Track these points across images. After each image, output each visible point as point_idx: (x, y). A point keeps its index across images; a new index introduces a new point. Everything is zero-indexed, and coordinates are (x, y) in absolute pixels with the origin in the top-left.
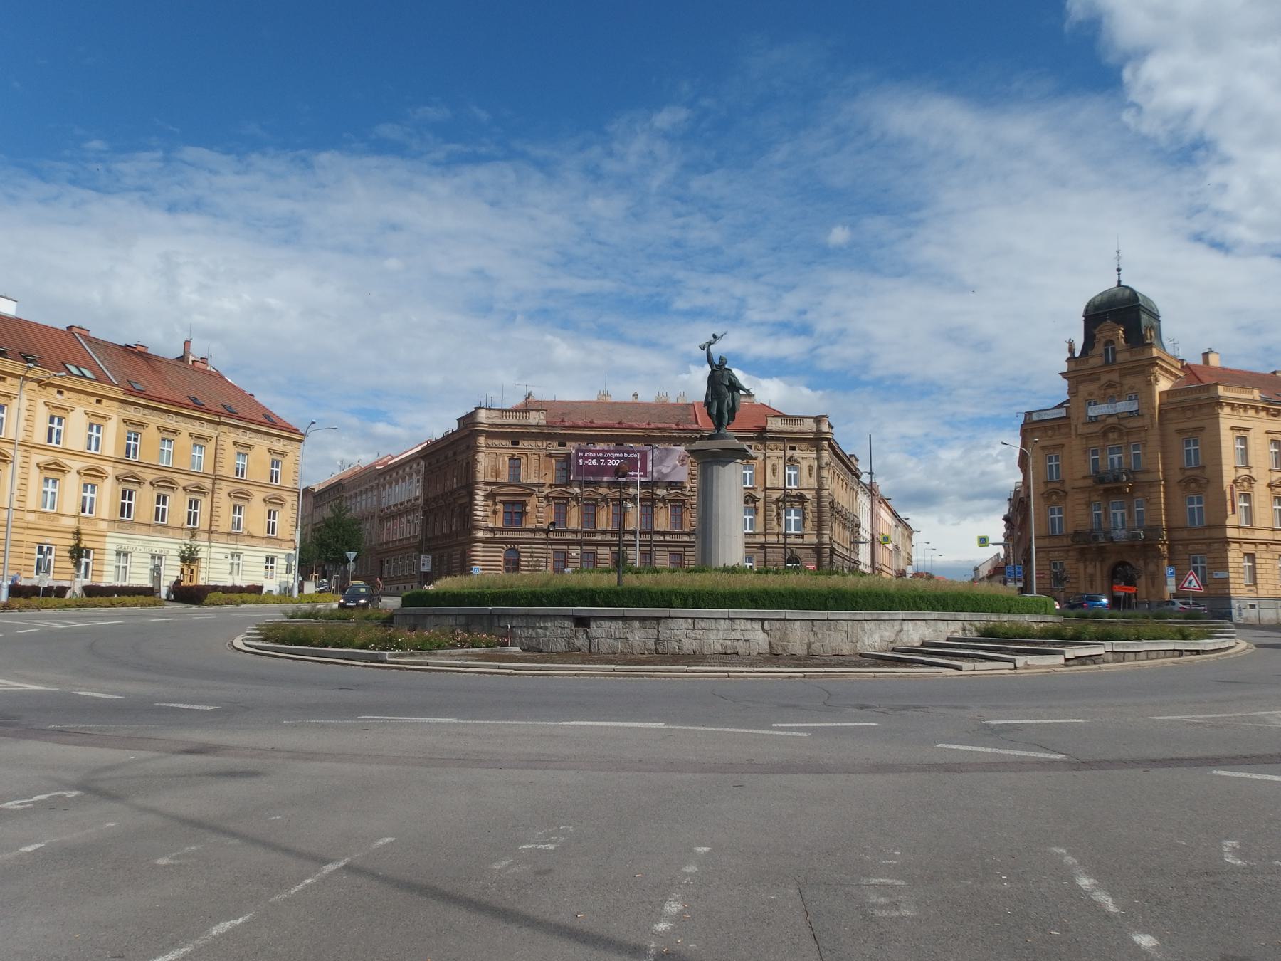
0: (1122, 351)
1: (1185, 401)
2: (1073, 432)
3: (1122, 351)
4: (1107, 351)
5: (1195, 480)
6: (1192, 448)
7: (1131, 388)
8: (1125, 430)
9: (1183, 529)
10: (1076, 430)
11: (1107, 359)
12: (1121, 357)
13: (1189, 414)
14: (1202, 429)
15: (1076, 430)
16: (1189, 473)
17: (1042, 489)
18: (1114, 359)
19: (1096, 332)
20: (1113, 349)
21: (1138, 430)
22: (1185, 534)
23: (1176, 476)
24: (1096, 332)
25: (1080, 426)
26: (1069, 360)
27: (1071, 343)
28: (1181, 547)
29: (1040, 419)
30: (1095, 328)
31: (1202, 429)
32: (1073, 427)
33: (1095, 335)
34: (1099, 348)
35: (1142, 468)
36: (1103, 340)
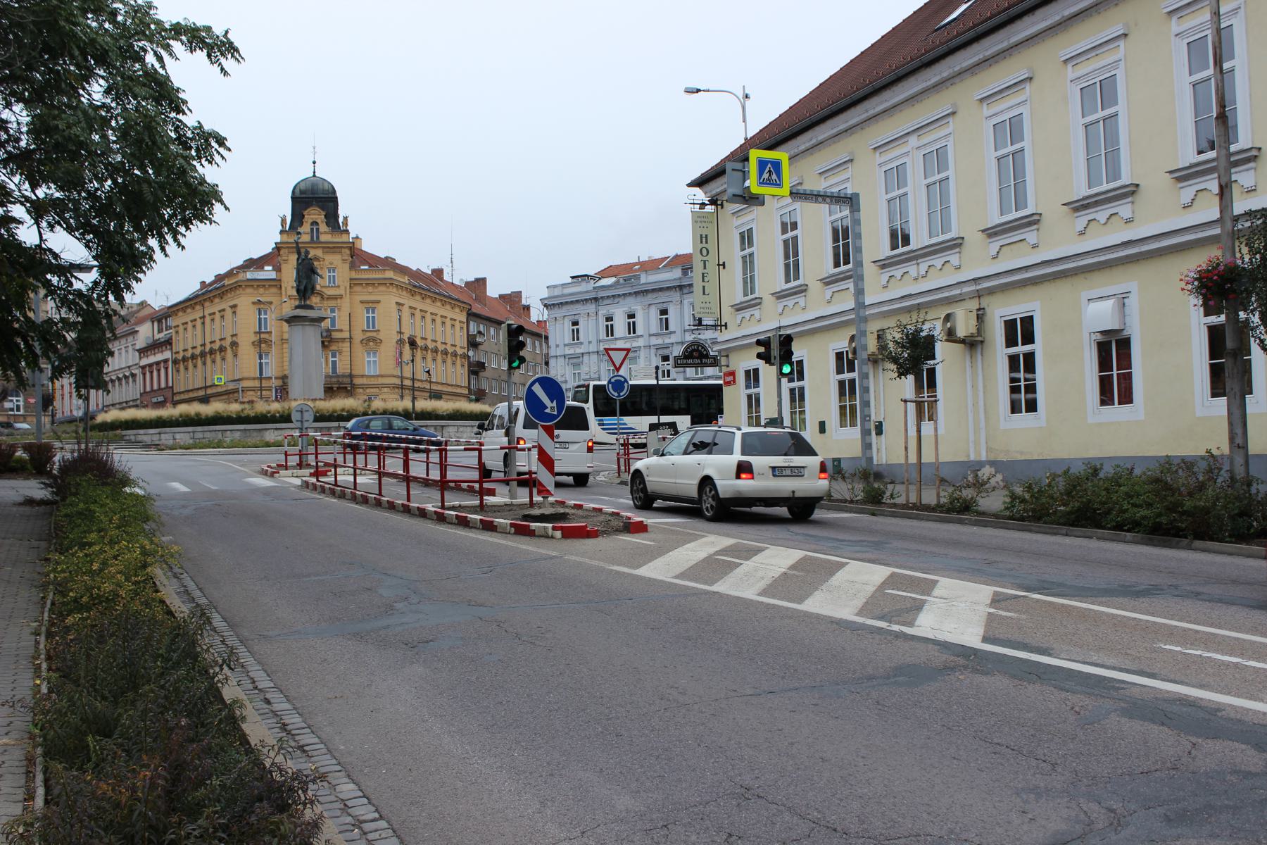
0: (325, 233)
1: (368, 279)
2: (284, 293)
3: (325, 233)
4: (312, 230)
5: (373, 339)
6: (371, 315)
7: (331, 264)
8: (326, 296)
9: (363, 376)
10: (286, 292)
11: (312, 237)
12: (323, 238)
13: (370, 289)
14: (378, 302)
15: (286, 292)
16: (369, 334)
17: (255, 338)
18: (318, 237)
19: (305, 213)
20: (318, 230)
21: (335, 298)
22: (364, 381)
23: (358, 336)
24: (305, 213)
25: (289, 288)
26: (282, 232)
27: (283, 221)
28: (361, 390)
29: (253, 278)
30: (306, 209)
31: (378, 302)
32: (283, 289)
33: (304, 216)
34: (305, 228)
35: (337, 328)
36: (310, 221)
